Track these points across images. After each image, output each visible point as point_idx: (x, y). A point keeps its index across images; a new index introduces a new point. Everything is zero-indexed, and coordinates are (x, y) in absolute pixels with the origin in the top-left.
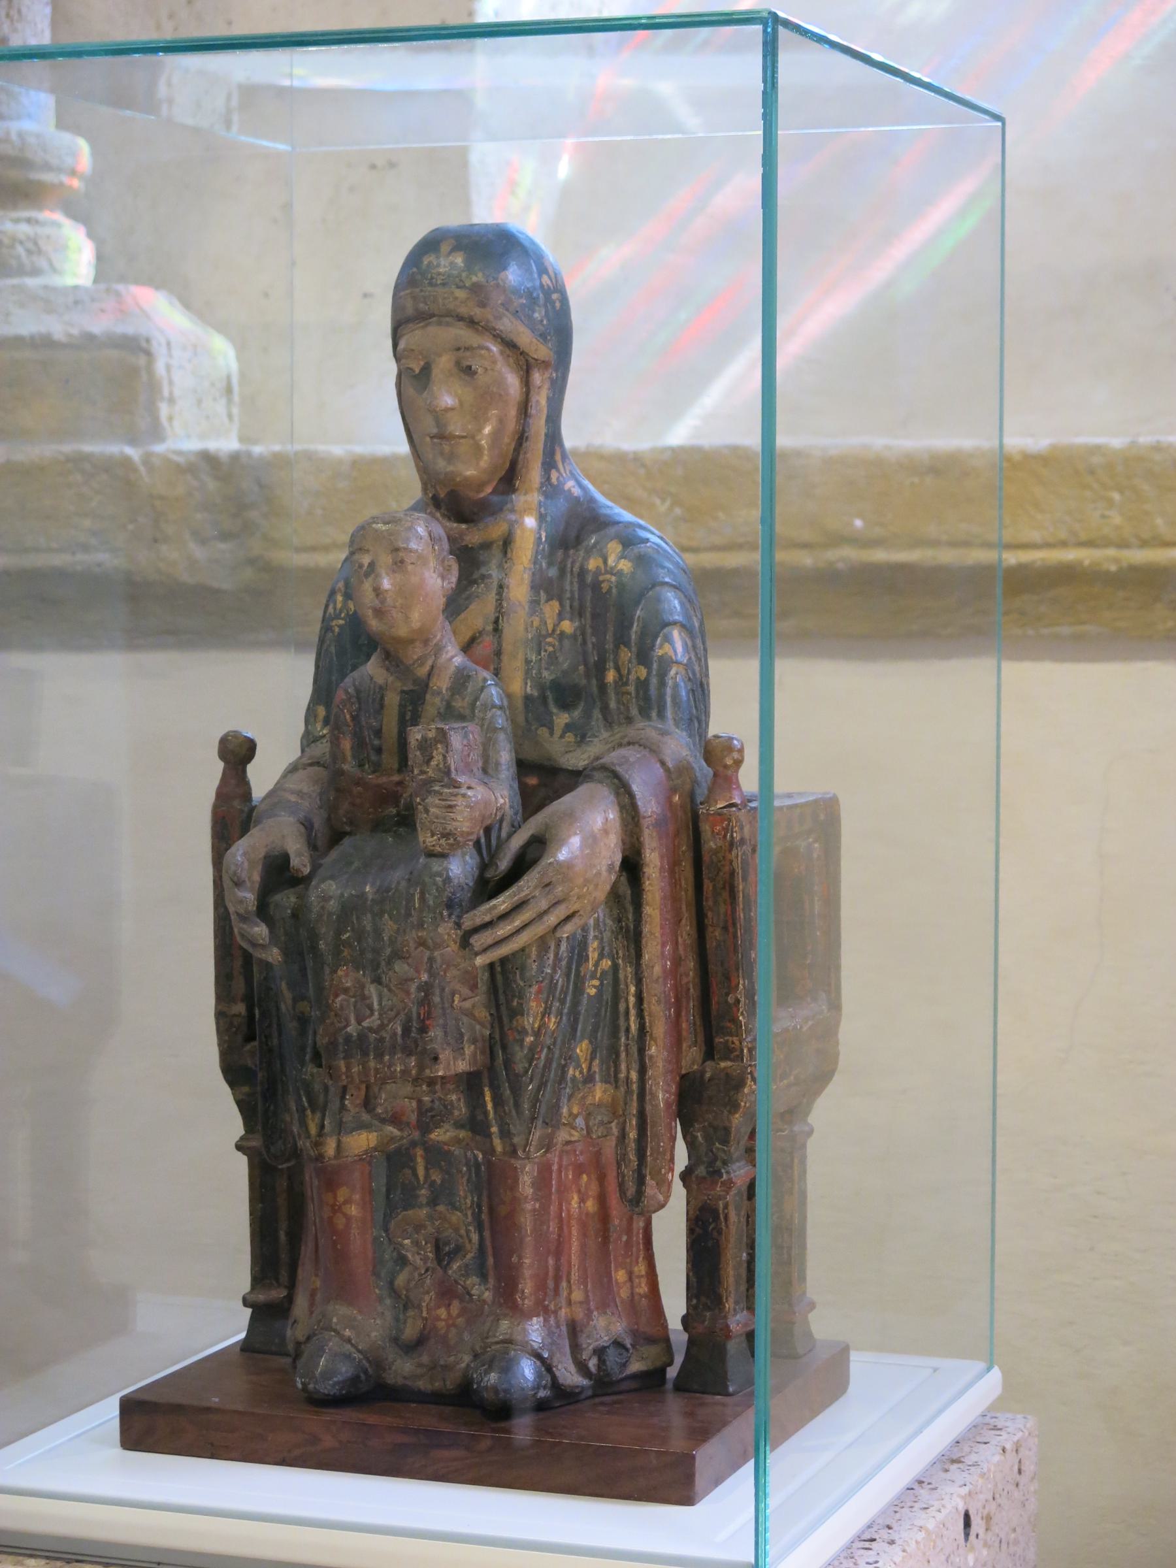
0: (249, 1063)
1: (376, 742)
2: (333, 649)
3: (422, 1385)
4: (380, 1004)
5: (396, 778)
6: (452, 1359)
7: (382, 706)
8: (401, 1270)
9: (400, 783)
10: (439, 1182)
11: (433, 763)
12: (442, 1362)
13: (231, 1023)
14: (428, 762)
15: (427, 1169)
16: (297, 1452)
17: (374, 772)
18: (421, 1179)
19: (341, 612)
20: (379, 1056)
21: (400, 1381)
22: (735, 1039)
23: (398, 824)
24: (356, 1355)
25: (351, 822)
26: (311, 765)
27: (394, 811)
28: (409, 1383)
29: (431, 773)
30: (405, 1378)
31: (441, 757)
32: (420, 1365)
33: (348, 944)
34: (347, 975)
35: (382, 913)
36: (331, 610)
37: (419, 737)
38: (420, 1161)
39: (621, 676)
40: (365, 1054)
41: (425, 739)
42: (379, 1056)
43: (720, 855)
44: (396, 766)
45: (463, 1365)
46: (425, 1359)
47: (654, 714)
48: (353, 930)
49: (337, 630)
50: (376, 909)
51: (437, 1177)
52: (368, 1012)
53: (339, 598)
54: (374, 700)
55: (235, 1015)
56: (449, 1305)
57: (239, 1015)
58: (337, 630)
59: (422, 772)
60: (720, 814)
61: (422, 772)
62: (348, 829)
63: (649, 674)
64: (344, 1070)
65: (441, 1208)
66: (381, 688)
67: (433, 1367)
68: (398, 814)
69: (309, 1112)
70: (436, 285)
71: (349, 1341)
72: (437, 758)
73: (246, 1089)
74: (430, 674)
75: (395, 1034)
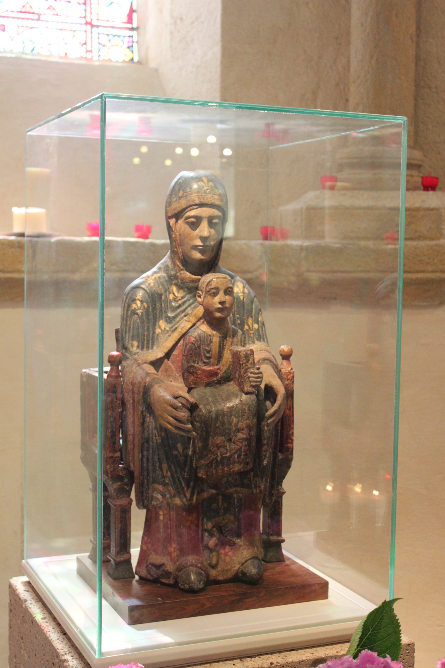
0: (121, 474)
1: (208, 355)
2: (138, 321)
3: (221, 578)
4: (230, 447)
5: (216, 367)
6: (229, 567)
7: (211, 342)
8: (210, 540)
9: (218, 369)
10: (226, 506)
11: (250, 362)
12: (226, 569)
13: (115, 460)
14: (248, 362)
15: (222, 503)
16: (197, 611)
17: (205, 366)
18: (220, 506)
19: (141, 307)
20: (228, 465)
21: (213, 578)
22: (291, 445)
23: (216, 383)
24: (203, 572)
25: (195, 384)
26: (145, 363)
27: (216, 379)
28: (215, 578)
29: (249, 366)
30: (214, 577)
31: (252, 360)
32: (218, 571)
33: (218, 427)
34: (217, 439)
35: (232, 415)
36: (134, 306)
37: (244, 353)
38: (220, 501)
39: (250, 328)
40: (223, 465)
41: (246, 354)
42: (228, 465)
43: (289, 386)
44: (216, 363)
45: (236, 568)
46: (219, 569)
47: (262, 340)
48: (220, 422)
49: (140, 314)
50: (228, 414)
51: (226, 505)
52: (226, 451)
53: (139, 303)
54: (207, 340)
55: (116, 457)
56: (225, 548)
57: (118, 457)
58: (140, 314)
59: (246, 365)
60: (290, 372)
61: (246, 365)
62: (193, 386)
63: (259, 327)
64: (214, 472)
65: (228, 515)
66: (210, 336)
67: (223, 570)
68: (217, 380)
69: (185, 488)
70: (207, 193)
71: (200, 568)
72: (251, 360)
73: (119, 483)
74: (227, 332)
75: (235, 457)
